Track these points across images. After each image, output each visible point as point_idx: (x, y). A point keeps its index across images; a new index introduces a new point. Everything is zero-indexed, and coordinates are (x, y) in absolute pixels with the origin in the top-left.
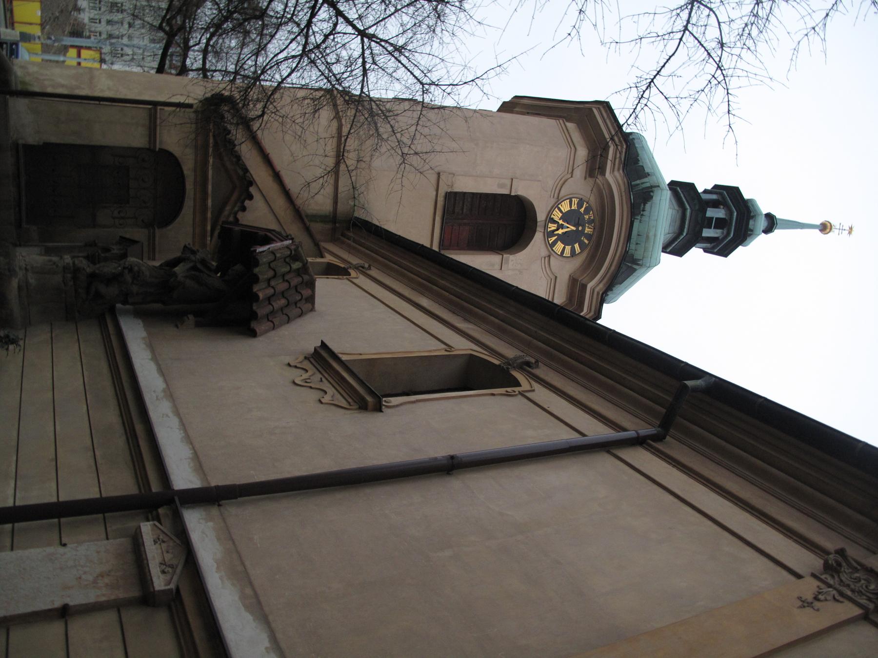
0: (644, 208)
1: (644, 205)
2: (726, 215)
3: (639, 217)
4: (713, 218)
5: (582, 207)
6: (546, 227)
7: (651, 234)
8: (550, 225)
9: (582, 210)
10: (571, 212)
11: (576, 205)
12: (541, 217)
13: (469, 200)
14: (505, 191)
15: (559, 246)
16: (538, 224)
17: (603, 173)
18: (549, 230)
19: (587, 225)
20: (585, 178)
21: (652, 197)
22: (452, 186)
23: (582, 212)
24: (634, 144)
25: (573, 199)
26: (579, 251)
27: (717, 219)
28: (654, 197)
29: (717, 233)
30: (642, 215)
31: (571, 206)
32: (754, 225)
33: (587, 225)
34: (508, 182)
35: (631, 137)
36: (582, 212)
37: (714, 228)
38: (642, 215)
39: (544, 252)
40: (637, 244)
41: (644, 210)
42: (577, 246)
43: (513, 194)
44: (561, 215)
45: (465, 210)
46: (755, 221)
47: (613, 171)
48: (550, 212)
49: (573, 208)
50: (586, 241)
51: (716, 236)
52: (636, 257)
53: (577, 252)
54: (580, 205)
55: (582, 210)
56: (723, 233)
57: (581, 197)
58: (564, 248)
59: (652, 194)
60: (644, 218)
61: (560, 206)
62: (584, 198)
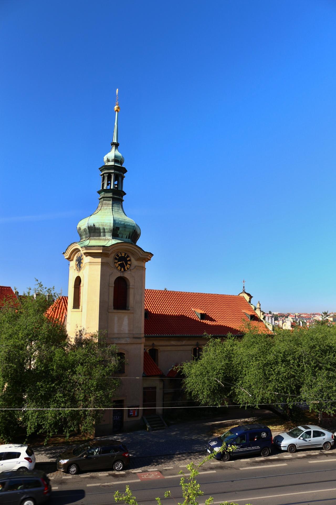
8: (122, 271)
9: (118, 258)
12: (119, 274)
39: (129, 272)
42: (128, 259)
43: (114, 286)
47: (109, 250)
50: (127, 255)
54: (116, 259)
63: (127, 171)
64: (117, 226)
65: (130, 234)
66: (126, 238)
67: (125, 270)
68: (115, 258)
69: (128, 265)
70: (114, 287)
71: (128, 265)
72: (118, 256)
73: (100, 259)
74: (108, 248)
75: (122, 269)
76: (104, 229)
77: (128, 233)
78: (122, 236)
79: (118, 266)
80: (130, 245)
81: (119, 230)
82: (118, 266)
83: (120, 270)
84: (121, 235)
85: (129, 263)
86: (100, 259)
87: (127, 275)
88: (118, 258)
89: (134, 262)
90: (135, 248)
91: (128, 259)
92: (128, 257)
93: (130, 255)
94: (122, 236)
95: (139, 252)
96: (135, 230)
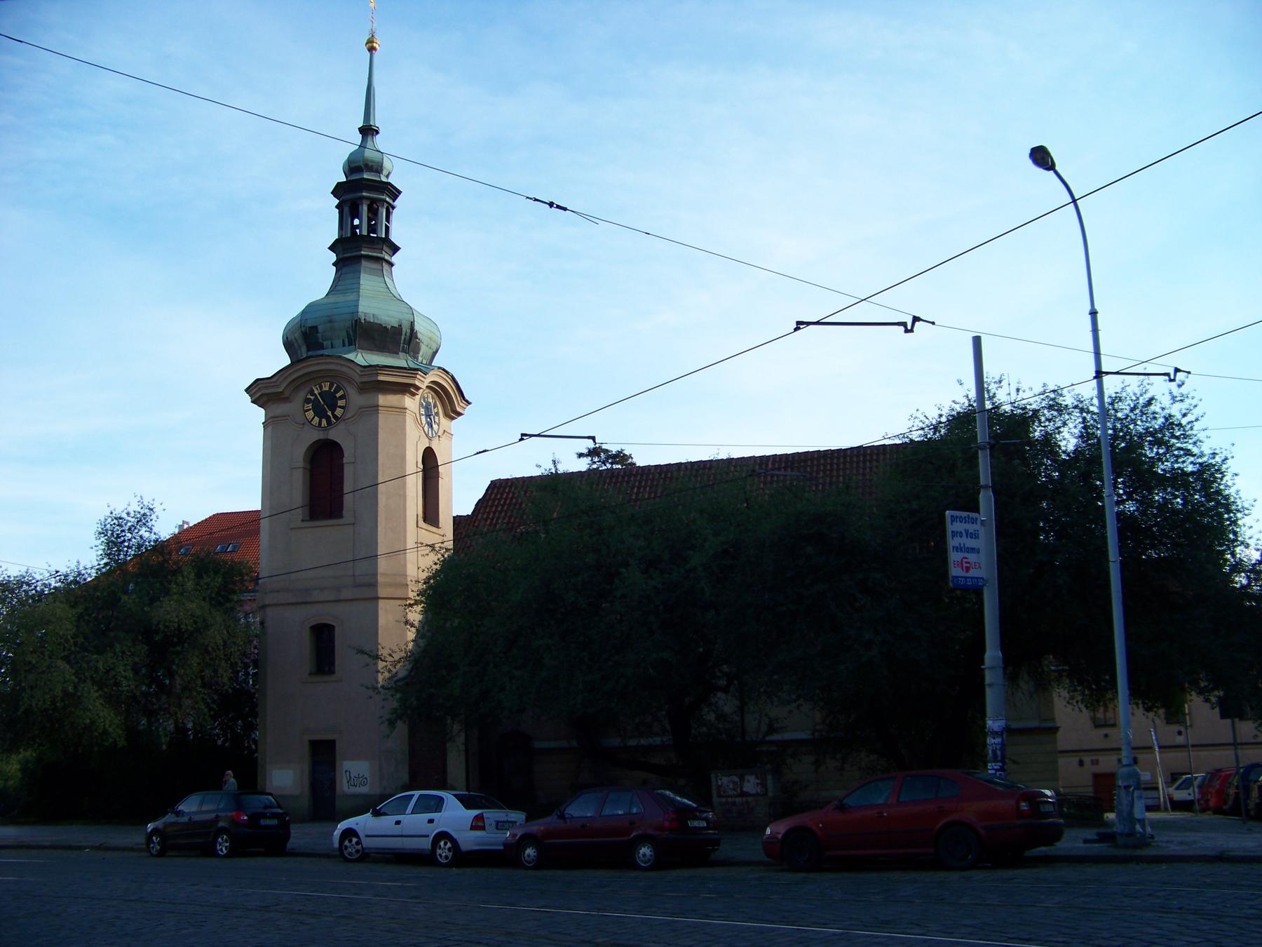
10: (313, 409)
12: (316, 436)
15: (339, 412)
25: (305, 409)
31: (310, 410)
39: (342, 426)
42: (338, 395)
49: (311, 407)
54: (307, 401)
58: (340, 407)
63: (332, 193)
64: (310, 326)
65: (348, 334)
66: (344, 345)
67: (329, 422)
74: (274, 379)
75: (324, 422)
76: (295, 338)
77: (344, 333)
78: (332, 344)
79: (314, 418)
80: (328, 361)
81: (318, 332)
82: (314, 418)
84: (329, 342)
85: (341, 403)
87: (335, 435)
88: (310, 397)
89: (357, 399)
90: (327, 363)
91: (338, 395)
93: (345, 384)
94: (332, 344)
95: (352, 369)
96: (356, 321)
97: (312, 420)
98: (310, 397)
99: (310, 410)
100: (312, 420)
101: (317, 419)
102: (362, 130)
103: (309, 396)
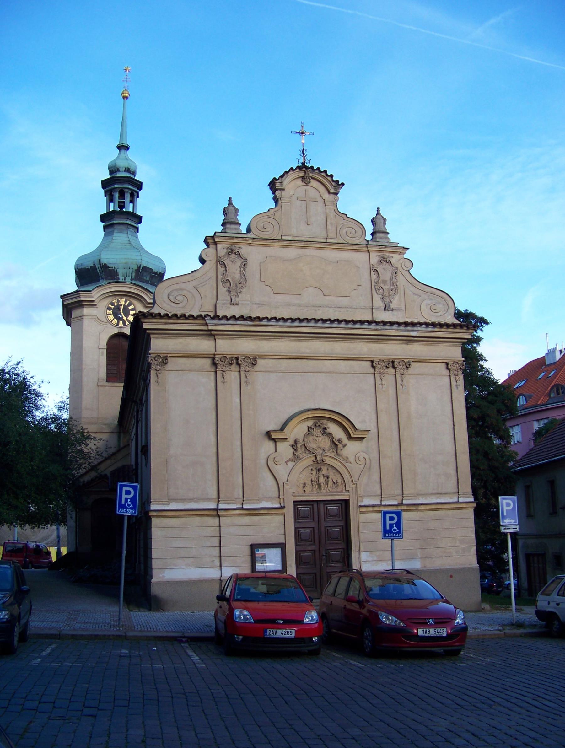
0: (111, 267)
1: (109, 267)
2: (117, 192)
3: (116, 269)
4: (119, 201)
5: (111, 305)
6: (121, 327)
7: (124, 261)
8: (120, 325)
9: (113, 307)
10: (113, 314)
11: (110, 311)
12: (116, 331)
13: (110, 366)
14: (105, 351)
16: (120, 332)
17: (94, 301)
18: (122, 325)
19: (120, 303)
20: (97, 307)
21: (105, 264)
22: (104, 379)
23: (113, 307)
24: (80, 269)
25: (108, 313)
26: (133, 305)
27: (119, 199)
28: (105, 263)
29: (127, 196)
30: (114, 268)
31: (111, 314)
32: (123, 167)
33: (120, 303)
34: (101, 350)
35: (77, 270)
36: (113, 307)
37: (124, 199)
38: (114, 268)
40: (129, 269)
41: (112, 268)
42: (130, 308)
43: (106, 348)
44: (115, 319)
45: (115, 368)
46: (120, 167)
47: (92, 296)
48: (113, 325)
49: (111, 313)
51: (129, 196)
52: (136, 269)
53: (133, 307)
54: (109, 309)
55: (113, 307)
56: (127, 192)
57: (106, 309)
59: (103, 264)
60: (116, 267)
61: (111, 321)
62: (107, 307)
68: (107, 308)
69: (130, 316)
70: (106, 349)
71: (130, 316)
72: (112, 304)
73: (144, 327)
75: (121, 323)
79: (113, 319)
82: (113, 319)
83: (116, 324)
86: (144, 327)
88: (111, 306)
92: (130, 304)
97: (112, 321)
98: (111, 306)
99: (111, 314)
100: (112, 321)
101: (115, 321)
102: (120, 147)
103: (110, 306)
